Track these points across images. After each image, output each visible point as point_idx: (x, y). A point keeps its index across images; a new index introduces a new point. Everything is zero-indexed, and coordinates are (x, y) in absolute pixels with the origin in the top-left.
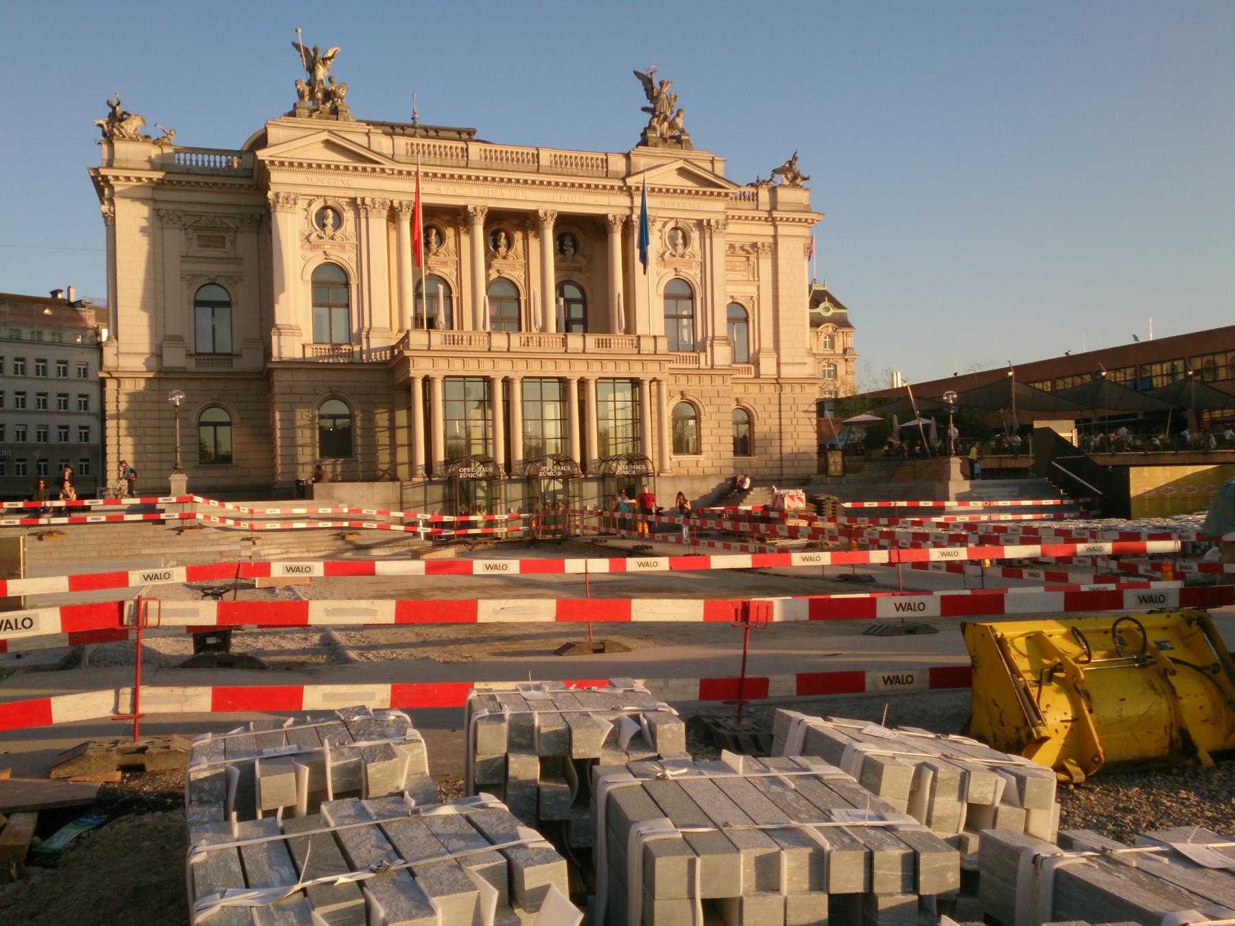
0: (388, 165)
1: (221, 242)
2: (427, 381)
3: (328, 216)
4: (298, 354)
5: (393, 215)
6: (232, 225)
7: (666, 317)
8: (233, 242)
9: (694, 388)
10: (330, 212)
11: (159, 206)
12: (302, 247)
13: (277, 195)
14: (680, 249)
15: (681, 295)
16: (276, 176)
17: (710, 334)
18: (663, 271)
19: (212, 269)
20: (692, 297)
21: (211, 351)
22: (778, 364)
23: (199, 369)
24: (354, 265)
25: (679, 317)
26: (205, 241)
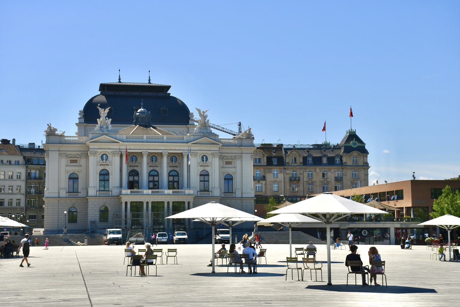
0: (121, 142)
1: (76, 161)
2: (126, 203)
3: (104, 157)
5: (121, 156)
7: (200, 181)
11: (60, 152)
14: (205, 162)
15: (205, 176)
16: (91, 147)
18: (200, 168)
19: (73, 169)
20: (208, 175)
21: (72, 191)
22: (242, 193)
25: (204, 181)
26: (72, 161)
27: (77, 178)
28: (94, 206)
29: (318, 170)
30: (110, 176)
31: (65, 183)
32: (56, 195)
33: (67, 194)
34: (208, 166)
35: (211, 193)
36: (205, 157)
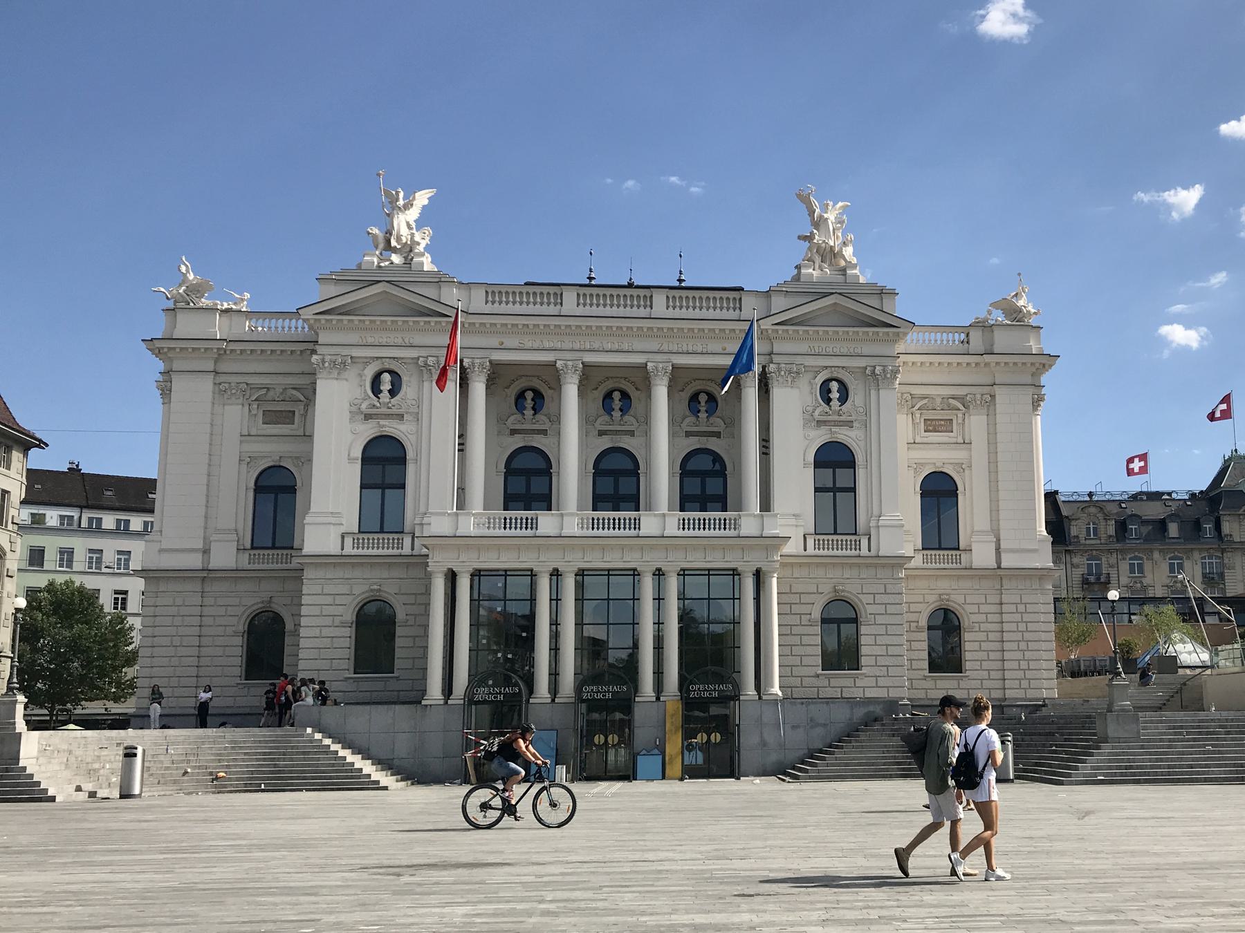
1: (286, 417)
2: (452, 577)
3: (385, 382)
4: (334, 548)
6: (302, 398)
7: (817, 490)
8: (305, 415)
9: (854, 587)
10: (386, 377)
12: (352, 420)
13: (323, 361)
15: (835, 461)
17: (876, 512)
20: (851, 463)
23: (251, 567)
24: (413, 438)
25: (835, 490)
26: (272, 417)
27: (292, 490)
28: (329, 600)
29: (1156, 555)
30: (411, 469)
31: (236, 507)
32: (195, 561)
33: (245, 557)
34: (849, 424)
35: (864, 542)
36: (834, 386)
